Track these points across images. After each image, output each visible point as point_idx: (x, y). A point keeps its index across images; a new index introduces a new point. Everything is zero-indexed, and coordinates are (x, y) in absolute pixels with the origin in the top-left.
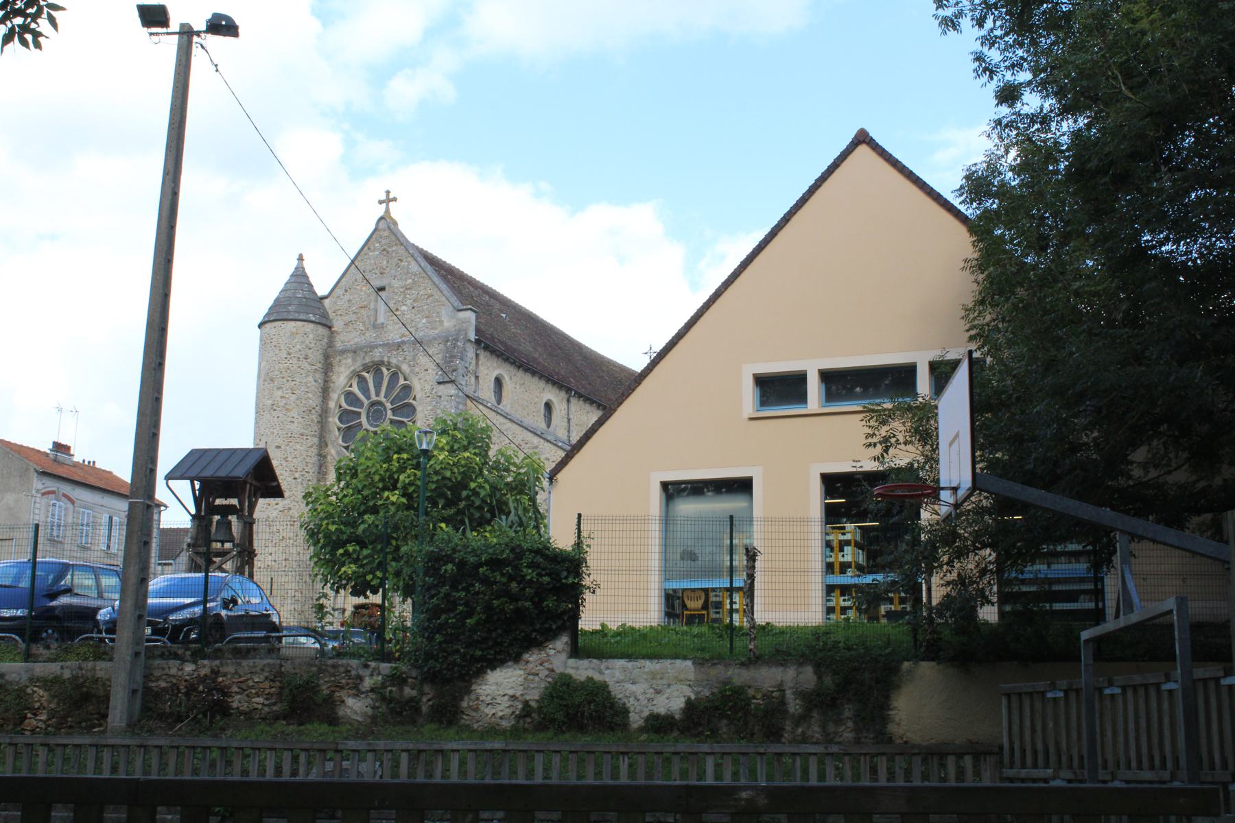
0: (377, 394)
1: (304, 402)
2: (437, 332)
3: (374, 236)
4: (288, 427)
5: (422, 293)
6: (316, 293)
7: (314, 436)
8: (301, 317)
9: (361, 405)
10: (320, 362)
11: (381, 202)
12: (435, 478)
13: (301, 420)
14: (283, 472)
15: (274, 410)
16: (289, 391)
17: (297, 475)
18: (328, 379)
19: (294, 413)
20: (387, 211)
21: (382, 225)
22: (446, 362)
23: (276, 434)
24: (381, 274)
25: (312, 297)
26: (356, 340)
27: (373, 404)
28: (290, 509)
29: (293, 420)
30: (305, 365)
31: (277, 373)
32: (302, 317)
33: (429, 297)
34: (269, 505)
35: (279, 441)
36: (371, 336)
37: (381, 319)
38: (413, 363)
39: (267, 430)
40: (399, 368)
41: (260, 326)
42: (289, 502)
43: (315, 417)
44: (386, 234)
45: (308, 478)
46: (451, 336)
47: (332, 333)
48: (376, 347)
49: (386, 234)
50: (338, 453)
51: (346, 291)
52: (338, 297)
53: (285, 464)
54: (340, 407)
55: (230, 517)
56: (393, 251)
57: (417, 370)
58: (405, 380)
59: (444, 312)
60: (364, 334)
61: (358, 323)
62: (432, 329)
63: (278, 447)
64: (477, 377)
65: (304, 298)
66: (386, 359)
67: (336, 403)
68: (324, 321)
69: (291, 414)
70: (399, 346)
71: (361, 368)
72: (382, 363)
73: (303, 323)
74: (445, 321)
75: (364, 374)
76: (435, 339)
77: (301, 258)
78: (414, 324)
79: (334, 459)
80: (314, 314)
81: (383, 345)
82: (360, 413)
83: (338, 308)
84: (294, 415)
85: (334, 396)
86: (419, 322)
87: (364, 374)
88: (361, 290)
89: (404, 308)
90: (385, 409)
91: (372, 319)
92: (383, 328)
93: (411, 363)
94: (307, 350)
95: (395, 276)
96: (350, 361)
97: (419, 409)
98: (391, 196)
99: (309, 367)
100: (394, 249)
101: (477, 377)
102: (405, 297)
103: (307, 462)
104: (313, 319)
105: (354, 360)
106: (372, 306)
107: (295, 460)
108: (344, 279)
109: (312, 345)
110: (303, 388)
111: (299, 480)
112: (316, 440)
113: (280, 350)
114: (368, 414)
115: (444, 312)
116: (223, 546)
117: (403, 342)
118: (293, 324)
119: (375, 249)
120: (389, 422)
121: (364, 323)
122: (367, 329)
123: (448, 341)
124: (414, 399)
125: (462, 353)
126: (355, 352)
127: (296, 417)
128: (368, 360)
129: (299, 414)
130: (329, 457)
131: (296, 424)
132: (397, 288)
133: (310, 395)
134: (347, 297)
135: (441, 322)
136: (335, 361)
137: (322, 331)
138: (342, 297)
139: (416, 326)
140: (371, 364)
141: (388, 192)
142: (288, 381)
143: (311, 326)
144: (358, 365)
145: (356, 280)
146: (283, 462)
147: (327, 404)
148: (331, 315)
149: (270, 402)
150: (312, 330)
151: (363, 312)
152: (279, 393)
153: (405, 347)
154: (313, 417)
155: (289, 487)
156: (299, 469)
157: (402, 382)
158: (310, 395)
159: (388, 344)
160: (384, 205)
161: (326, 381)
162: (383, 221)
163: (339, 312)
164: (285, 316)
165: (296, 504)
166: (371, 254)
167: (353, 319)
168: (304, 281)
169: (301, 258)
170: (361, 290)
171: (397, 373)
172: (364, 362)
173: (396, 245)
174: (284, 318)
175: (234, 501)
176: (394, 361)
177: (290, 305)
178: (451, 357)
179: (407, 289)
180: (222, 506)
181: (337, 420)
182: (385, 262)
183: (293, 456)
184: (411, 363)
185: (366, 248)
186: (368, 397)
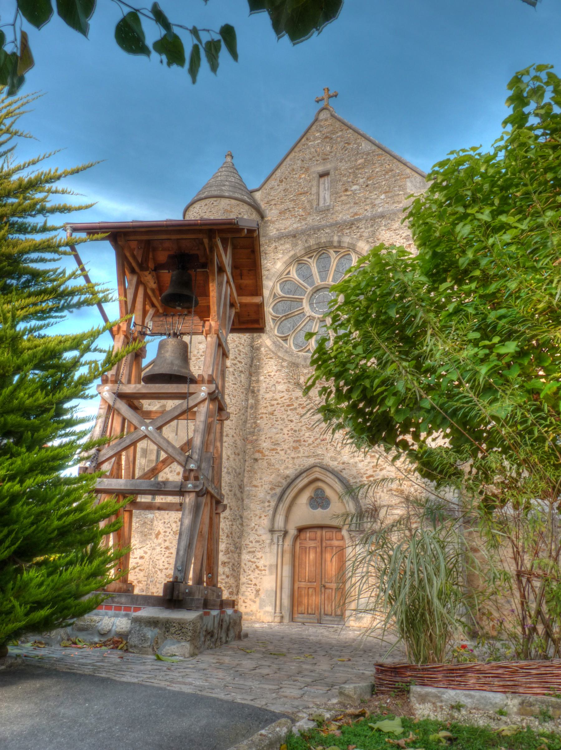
24: (324, 160)
26: (295, 226)
33: (387, 173)
36: (314, 220)
45: (240, 369)
56: (338, 137)
60: (305, 219)
62: (394, 203)
70: (353, 224)
73: (238, 202)
75: (305, 258)
78: (368, 201)
79: (270, 350)
81: (331, 225)
82: (302, 299)
83: (271, 198)
86: (375, 199)
88: (300, 178)
89: (355, 187)
91: (315, 203)
93: (370, 240)
98: (331, 93)
102: (356, 176)
103: (239, 350)
105: (295, 245)
108: (279, 171)
117: (359, 220)
118: (227, 201)
119: (316, 138)
121: (304, 209)
122: (309, 214)
126: (294, 236)
128: (312, 242)
130: (262, 349)
139: (372, 203)
144: (299, 250)
145: (293, 170)
151: (303, 198)
153: (360, 225)
172: (306, 245)
173: (342, 131)
179: (357, 169)
182: (328, 148)
184: (370, 240)
186: (312, 283)
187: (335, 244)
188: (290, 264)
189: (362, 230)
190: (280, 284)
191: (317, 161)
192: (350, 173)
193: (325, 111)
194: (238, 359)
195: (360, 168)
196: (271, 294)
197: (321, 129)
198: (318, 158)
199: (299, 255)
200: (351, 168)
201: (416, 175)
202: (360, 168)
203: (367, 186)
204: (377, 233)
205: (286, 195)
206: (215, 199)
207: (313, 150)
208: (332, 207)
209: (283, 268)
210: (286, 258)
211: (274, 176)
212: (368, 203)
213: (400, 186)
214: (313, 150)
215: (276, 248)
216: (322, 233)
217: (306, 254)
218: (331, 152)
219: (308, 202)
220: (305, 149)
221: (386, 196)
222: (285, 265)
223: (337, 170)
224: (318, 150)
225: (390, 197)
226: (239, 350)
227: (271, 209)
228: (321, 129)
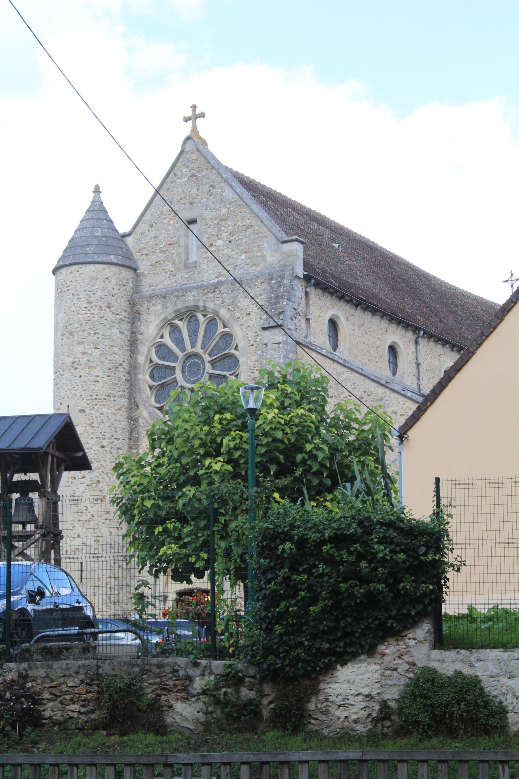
0: (193, 345)
1: (109, 358)
2: (258, 269)
3: (181, 160)
4: (92, 387)
5: (239, 224)
6: (117, 231)
7: (123, 396)
8: (100, 260)
9: (175, 359)
10: (125, 311)
11: (186, 120)
12: (265, 441)
13: (106, 378)
14: (89, 440)
15: (76, 369)
16: (92, 346)
17: (105, 443)
18: (135, 330)
19: (98, 371)
20: (194, 129)
21: (190, 146)
22: (271, 304)
23: (79, 395)
24: (191, 204)
25: (112, 235)
26: (166, 283)
27: (189, 357)
28: (99, 482)
29: (98, 379)
30: (108, 314)
31: (77, 325)
32: (102, 259)
33: (247, 228)
34: (75, 478)
35: (83, 405)
36: (182, 277)
37: (193, 257)
38: (233, 307)
39: (68, 393)
40: (216, 313)
41: (54, 272)
42: (98, 474)
43: (122, 374)
44: (194, 156)
45: (118, 446)
46: (276, 273)
47: (138, 276)
48: (189, 290)
49: (194, 156)
50: (150, 414)
51: (151, 226)
52: (142, 234)
53: (90, 431)
54: (151, 361)
55: (31, 495)
56: (203, 177)
57: (238, 314)
58: (225, 326)
59: (265, 245)
60: (174, 276)
61: (166, 262)
62: (252, 265)
63: (82, 411)
64: (308, 320)
65: (103, 237)
66: (201, 304)
67: (146, 357)
68: (128, 263)
69: (96, 372)
70: (216, 288)
71: (173, 315)
72: (196, 308)
74: (268, 255)
75: (177, 322)
76: (257, 277)
77: (97, 191)
79: (147, 422)
80: (116, 255)
81: (197, 288)
82: (174, 367)
83: (143, 246)
84: (98, 374)
85: (143, 349)
86: (237, 259)
87: (177, 322)
88: (169, 225)
89: (219, 242)
90: (203, 361)
91: (183, 258)
92: (195, 267)
93: (230, 307)
94: (110, 297)
95: (208, 206)
96: (159, 307)
97: (242, 360)
98: (198, 112)
99: (113, 317)
100: (204, 173)
101: (308, 320)
102: (220, 230)
103: (115, 428)
104: (115, 260)
105: (165, 307)
106: (182, 242)
107: (101, 426)
108: (148, 212)
109: (114, 292)
110: (107, 342)
111: (108, 449)
112: (125, 401)
113: (80, 298)
114: (183, 367)
115: (265, 245)
116: (24, 528)
117: (220, 283)
118: (91, 267)
120: (208, 376)
121: (173, 263)
122: (178, 270)
123: (272, 279)
124: (236, 348)
125: (288, 292)
126: (165, 297)
127: (101, 375)
128: (180, 305)
129: (104, 372)
130: (140, 421)
131: (101, 384)
132: (210, 219)
133: (116, 350)
134: (153, 233)
135: (263, 256)
136: (143, 309)
137: (126, 274)
138: (147, 233)
140: (184, 310)
141: (194, 107)
142: (89, 334)
143: (113, 268)
144: (169, 313)
145: (162, 213)
146: (88, 428)
147: (136, 359)
148: (136, 256)
149: (70, 359)
150: (114, 274)
152: (81, 349)
153: (223, 288)
154: (121, 374)
155: (96, 456)
156: (108, 436)
157: (221, 329)
158: (116, 350)
159: (203, 286)
160: (190, 123)
161: (133, 333)
162: (190, 142)
163: (145, 252)
164: (82, 259)
165: (105, 476)
166: (178, 181)
167: (161, 258)
168: (102, 216)
169: (97, 191)
170: (169, 225)
171: (215, 319)
172: (176, 308)
173: (207, 169)
174: (82, 261)
175: (35, 476)
176: (210, 305)
177: (88, 245)
178: (277, 297)
179: (221, 220)
180: (22, 481)
181: (148, 378)
182: (195, 190)
183: (99, 421)
184: (230, 307)
185: (172, 175)
186: (183, 349)
187: (202, 309)
188: (162, 327)
189: (224, 295)
190: (156, 348)
191: (185, 204)
192: (215, 224)
193: (190, 140)
194: (115, 437)
195: (224, 220)
196: (146, 360)
197: (188, 164)
198: (185, 201)
199: (169, 318)
200: (216, 219)
201: (271, 235)
202: (224, 220)
203: (230, 242)
204: (237, 301)
205: (156, 244)
206: (80, 266)
207: (180, 190)
208: (198, 264)
209: (156, 331)
210: (158, 321)
211: (144, 218)
212: (230, 262)
213: (258, 246)
214: (180, 190)
215: (148, 309)
216: (189, 296)
217: (176, 317)
218: (197, 196)
219: (177, 255)
220: (173, 187)
221: (246, 257)
222: (157, 329)
223: (203, 219)
224: (185, 190)
225: (250, 258)
226: (115, 428)
227: (143, 260)
228: (188, 164)
